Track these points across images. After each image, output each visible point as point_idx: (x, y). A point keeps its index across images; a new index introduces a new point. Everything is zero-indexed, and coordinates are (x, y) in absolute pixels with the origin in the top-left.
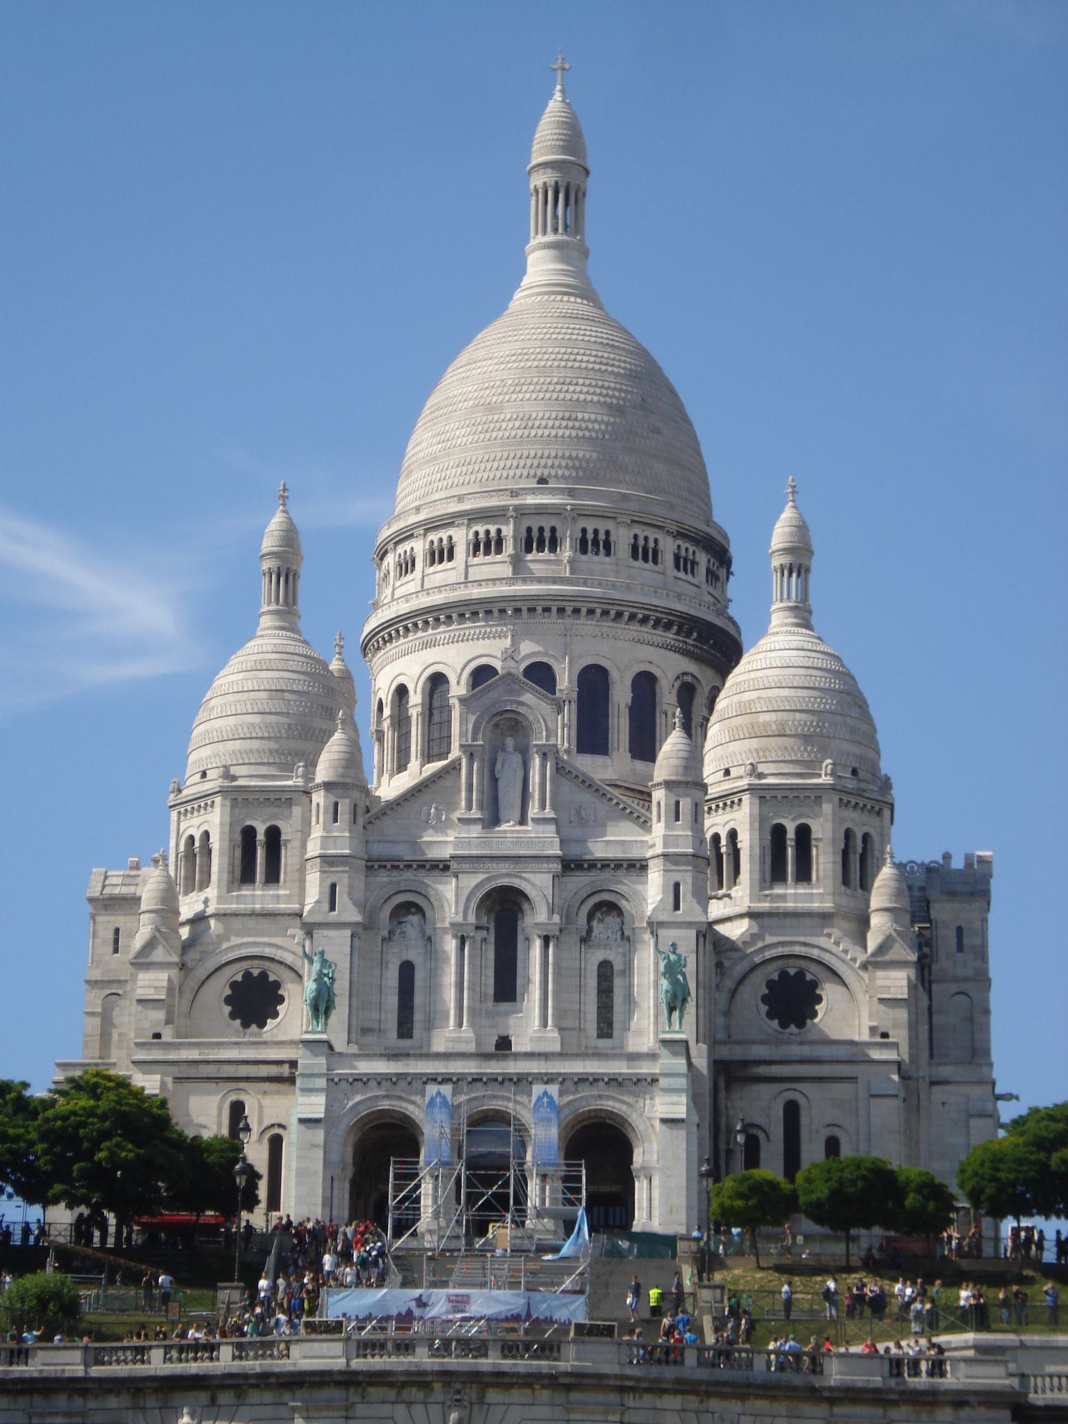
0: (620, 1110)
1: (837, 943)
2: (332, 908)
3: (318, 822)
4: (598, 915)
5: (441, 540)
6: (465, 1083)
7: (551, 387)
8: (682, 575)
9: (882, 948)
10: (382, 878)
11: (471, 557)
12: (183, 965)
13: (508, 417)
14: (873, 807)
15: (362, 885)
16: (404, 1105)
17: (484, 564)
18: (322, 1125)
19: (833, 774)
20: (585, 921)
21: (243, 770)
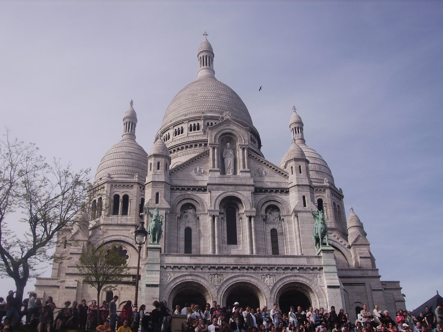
0: (306, 282)
1: (338, 239)
2: (157, 202)
3: (151, 170)
4: (269, 211)
5: (179, 128)
6: (229, 269)
7: (212, 90)
8: (253, 143)
9: (356, 240)
10: (178, 193)
11: (189, 132)
12: (89, 243)
13: (200, 96)
14: (339, 197)
15: (169, 195)
16: (199, 279)
17: (194, 133)
18: (158, 289)
19: (328, 182)
20: (264, 212)
21: (116, 176)
